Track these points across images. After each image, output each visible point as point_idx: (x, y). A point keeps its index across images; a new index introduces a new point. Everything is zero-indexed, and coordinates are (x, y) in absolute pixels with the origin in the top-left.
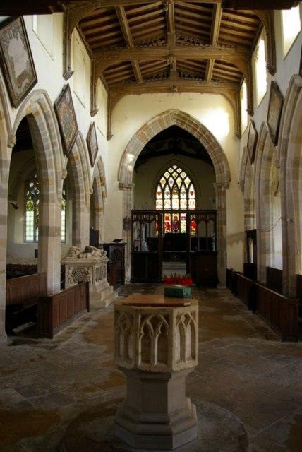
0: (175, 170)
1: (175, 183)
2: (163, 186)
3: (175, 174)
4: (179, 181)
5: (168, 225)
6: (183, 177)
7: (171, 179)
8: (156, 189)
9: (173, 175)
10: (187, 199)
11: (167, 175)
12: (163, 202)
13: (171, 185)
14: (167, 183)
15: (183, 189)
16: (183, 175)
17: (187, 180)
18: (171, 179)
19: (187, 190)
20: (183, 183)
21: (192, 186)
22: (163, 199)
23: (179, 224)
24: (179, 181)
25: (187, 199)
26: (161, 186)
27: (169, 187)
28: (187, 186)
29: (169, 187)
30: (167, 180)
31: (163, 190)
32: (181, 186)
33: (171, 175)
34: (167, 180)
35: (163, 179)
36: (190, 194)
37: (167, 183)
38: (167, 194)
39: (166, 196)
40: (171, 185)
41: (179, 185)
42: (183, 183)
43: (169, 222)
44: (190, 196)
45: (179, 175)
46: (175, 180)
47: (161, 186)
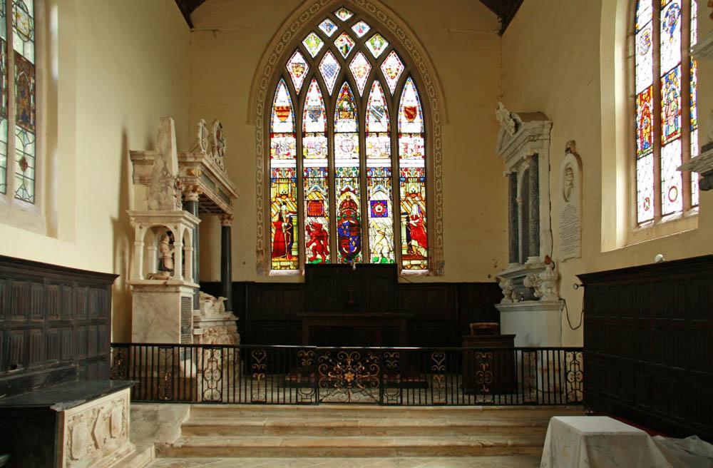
0: (345, 28)
1: (345, 77)
2: (298, 83)
3: (342, 42)
4: (360, 67)
5: (319, 234)
6: (376, 54)
7: (329, 60)
8: (271, 96)
9: (338, 44)
10: (394, 134)
11: (313, 45)
12: (299, 147)
13: (330, 82)
14: (314, 74)
15: (376, 96)
16: (377, 46)
17: (392, 66)
18: (329, 60)
19: (392, 101)
20: (376, 74)
21: (409, 86)
22: (299, 133)
23: (359, 230)
24: (360, 67)
25: (394, 134)
26: (290, 87)
27: (322, 87)
28: (392, 84)
29: (322, 87)
30: (314, 63)
31: (298, 99)
32: (369, 87)
33: (329, 46)
34: (314, 63)
35: (298, 58)
36: (402, 116)
37: (314, 74)
38: (315, 114)
39: (310, 125)
40: (330, 82)
41: (361, 83)
42: (376, 74)
43: (322, 221)
44: (405, 126)
45: (360, 47)
46: (344, 63)
47: (290, 87)
